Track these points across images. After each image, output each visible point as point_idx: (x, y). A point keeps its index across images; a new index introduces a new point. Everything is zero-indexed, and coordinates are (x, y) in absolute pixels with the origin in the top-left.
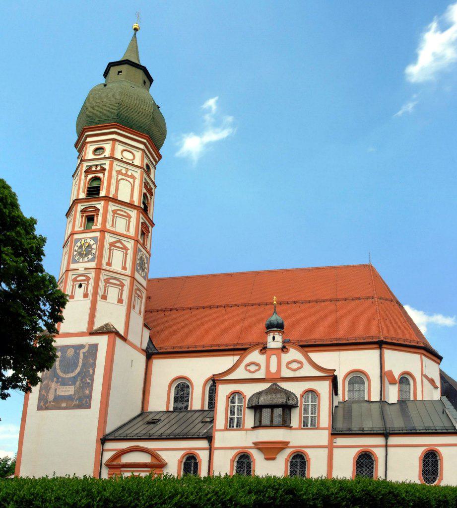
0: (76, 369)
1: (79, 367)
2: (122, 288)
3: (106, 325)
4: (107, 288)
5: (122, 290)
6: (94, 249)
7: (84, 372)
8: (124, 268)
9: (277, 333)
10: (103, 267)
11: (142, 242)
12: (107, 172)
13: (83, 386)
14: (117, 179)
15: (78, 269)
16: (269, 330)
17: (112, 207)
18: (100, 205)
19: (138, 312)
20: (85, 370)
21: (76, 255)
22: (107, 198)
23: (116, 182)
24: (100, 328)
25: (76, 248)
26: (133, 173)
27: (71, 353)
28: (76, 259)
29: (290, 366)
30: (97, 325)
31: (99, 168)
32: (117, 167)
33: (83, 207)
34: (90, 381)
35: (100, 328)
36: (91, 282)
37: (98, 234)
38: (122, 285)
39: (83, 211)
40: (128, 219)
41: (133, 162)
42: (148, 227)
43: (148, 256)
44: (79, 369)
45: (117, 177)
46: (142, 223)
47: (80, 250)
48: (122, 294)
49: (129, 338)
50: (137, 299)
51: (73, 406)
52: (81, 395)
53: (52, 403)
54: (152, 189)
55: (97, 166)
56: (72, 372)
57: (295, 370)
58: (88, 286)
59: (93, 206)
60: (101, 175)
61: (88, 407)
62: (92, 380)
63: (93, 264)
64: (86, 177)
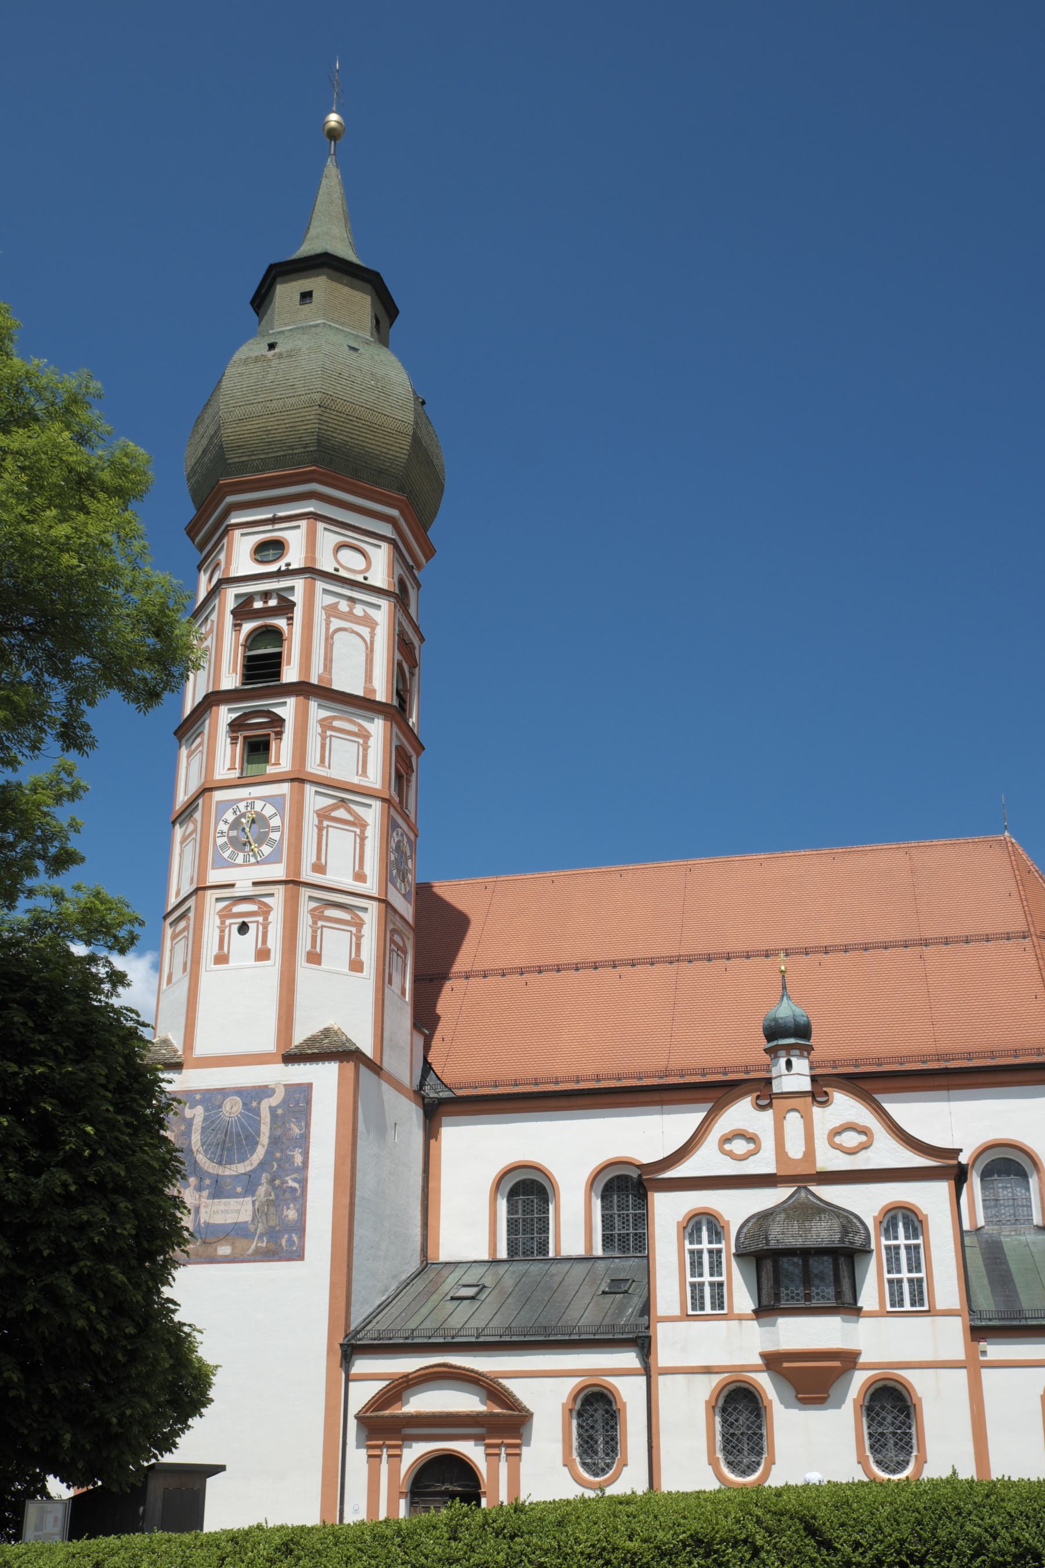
0: (253, 1150)
2: (359, 931)
3: (327, 1032)
4: (319, 932)
5: (359, 938)
6: (276, 829)
7: (279, 1161)
8: (360, 877)
9: (797, 1052)
10: (304, 878)
11: (397, 799)
12: (298, 613)
13: (277, 1196)
14: (327, 629)
15: (232, 886)
16: (775, 1043)
17: (316, 711)
18: (287, 709)
19: (398, 992)
20: (278, 1155)
21: (224, 846)
22: (303, 689)
23: (327, 639)
24: (309, 1039)
25: (223, 827)
26: (371, 612)
27: (234, 1109)
28: (226, 855)
29: (838, 1140)
30: (300, 1036)
31: (273, 603)
32: (323, 595)
33: (234, 716)
34: (296, 1185)
35: (311, 1041)
36: (276, 918)
37: (285, 788)
38: (359, 924)
39: (235, 726)
40: (361, 741)
41: (366, 578)
42: (409, 758)
43: (412, 836)
44: (260, 1153)
45: (328, 624)
46: (397, 747)
47: (233, 833)
48: (358, 946)
49: (386, 1066)
50: (395, 955)
51: (252, 1255)
52: (272, 1223)
54: (414, 648)
55: (266, 595)
56: (242, 1160)
57: (851, 1152)
58: (265, 928)
59: (266, 709)
60: (281, 623)
61: (297, 1255)
62: (303, 1182)
63: (278, 871)
64: (237, 626)
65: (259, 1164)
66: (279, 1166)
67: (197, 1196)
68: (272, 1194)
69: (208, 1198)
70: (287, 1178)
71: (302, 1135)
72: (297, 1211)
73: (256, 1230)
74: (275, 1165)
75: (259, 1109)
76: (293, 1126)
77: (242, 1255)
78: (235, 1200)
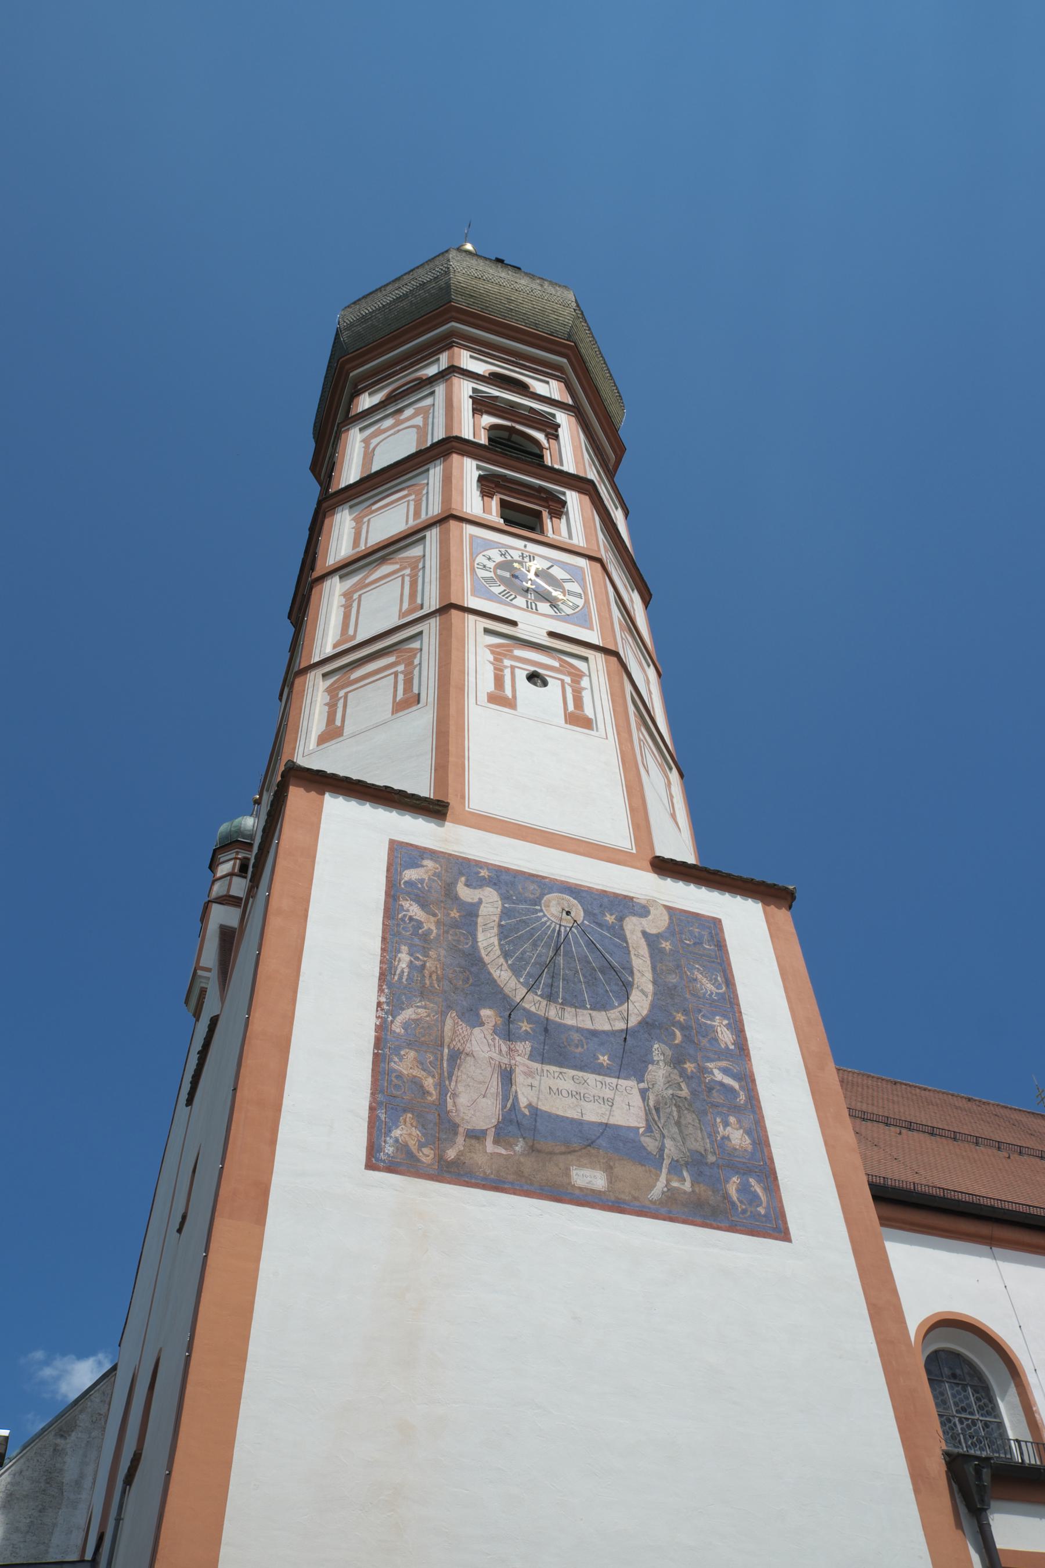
1: (635, 995)
13: (694, 1093)
20: (680, 1017)
53: (490, 1147)
65: (640, 1023)
66: (688, 1038)
67: (504, 1049)
68: (683, 1085)
69: (531, 1058)
70: (708, 1064)
71: (722, 996)
72: (748, 1132)
73: (662, 1149)
74: (678, 1033)
75: (622, 928)
76: (700, 976)
77: (636, 1199)
78: (600, 1078)
